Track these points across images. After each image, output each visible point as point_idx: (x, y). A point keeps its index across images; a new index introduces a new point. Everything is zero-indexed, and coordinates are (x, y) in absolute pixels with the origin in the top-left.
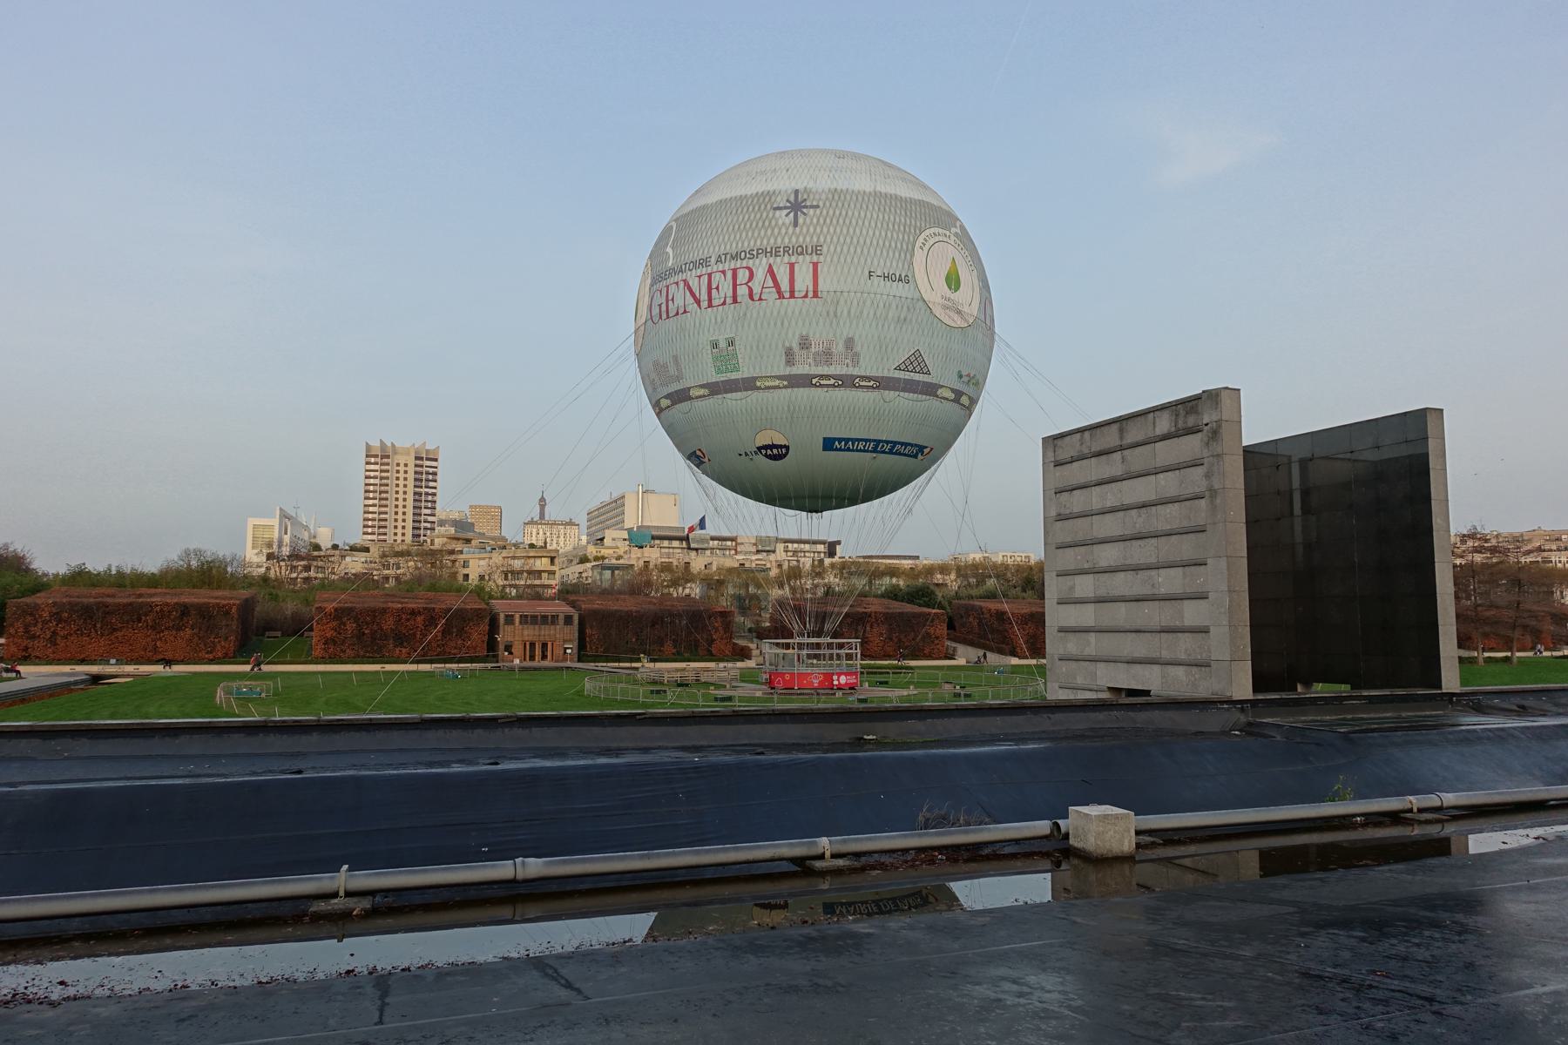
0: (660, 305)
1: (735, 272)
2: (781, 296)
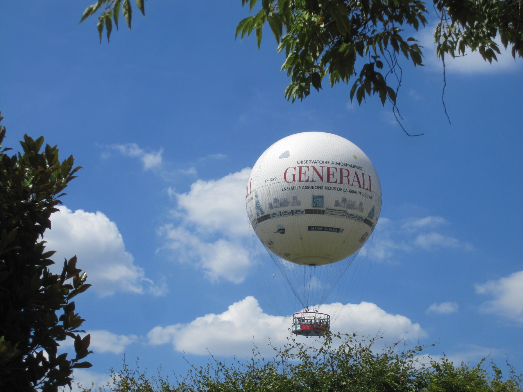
0: (294, 175)
1: (341, 170)
2: (360, 187)
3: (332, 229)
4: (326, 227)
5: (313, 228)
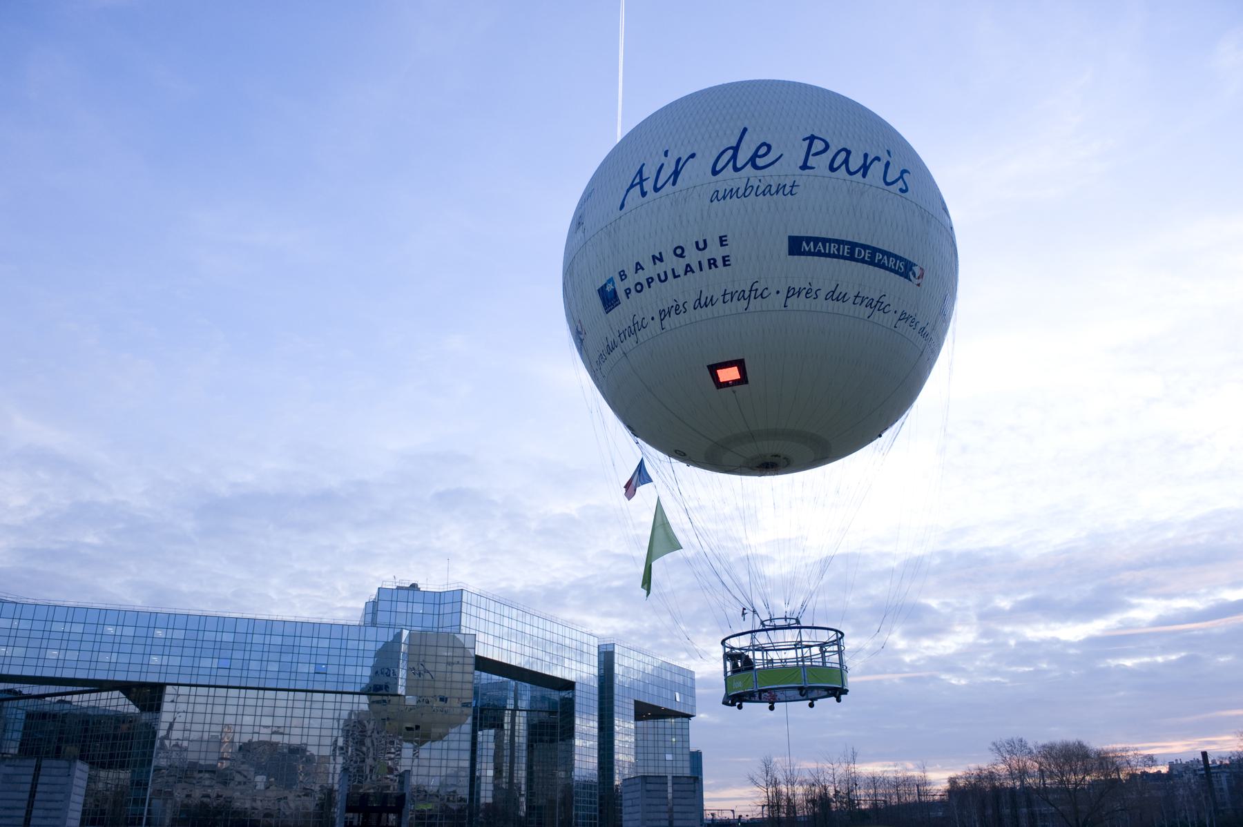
3: (885, 257)
4: (865, 247)
5: (812, 244)
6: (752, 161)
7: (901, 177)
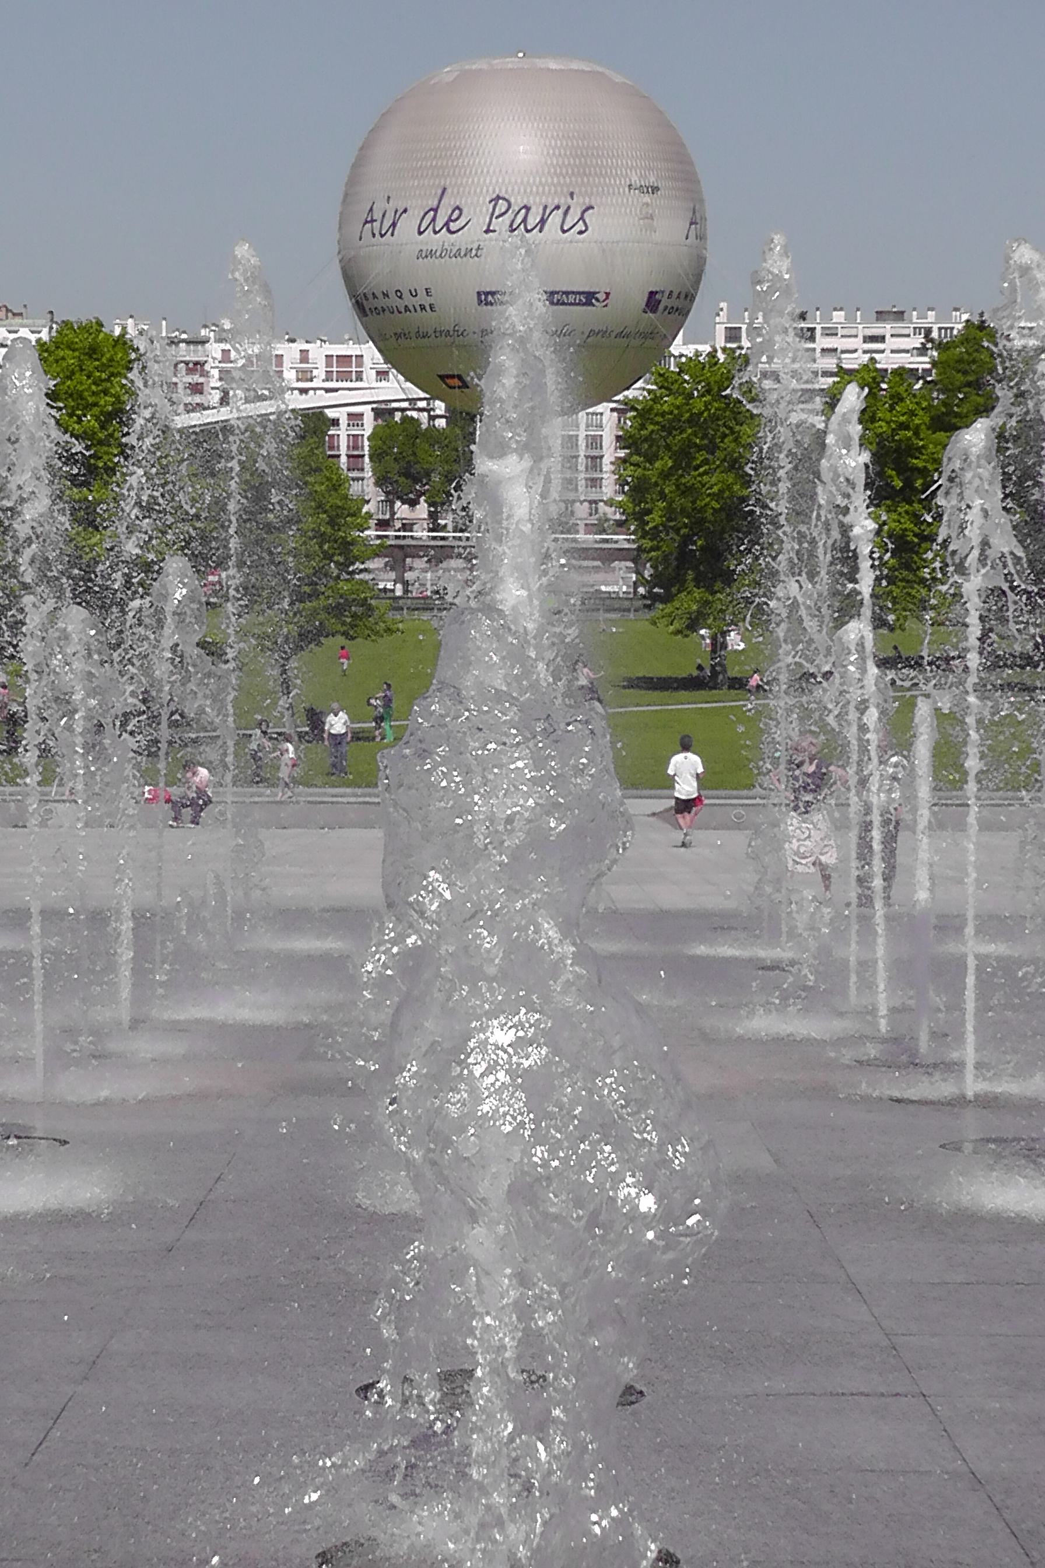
6: (447, 224)
7: (582, 218)
